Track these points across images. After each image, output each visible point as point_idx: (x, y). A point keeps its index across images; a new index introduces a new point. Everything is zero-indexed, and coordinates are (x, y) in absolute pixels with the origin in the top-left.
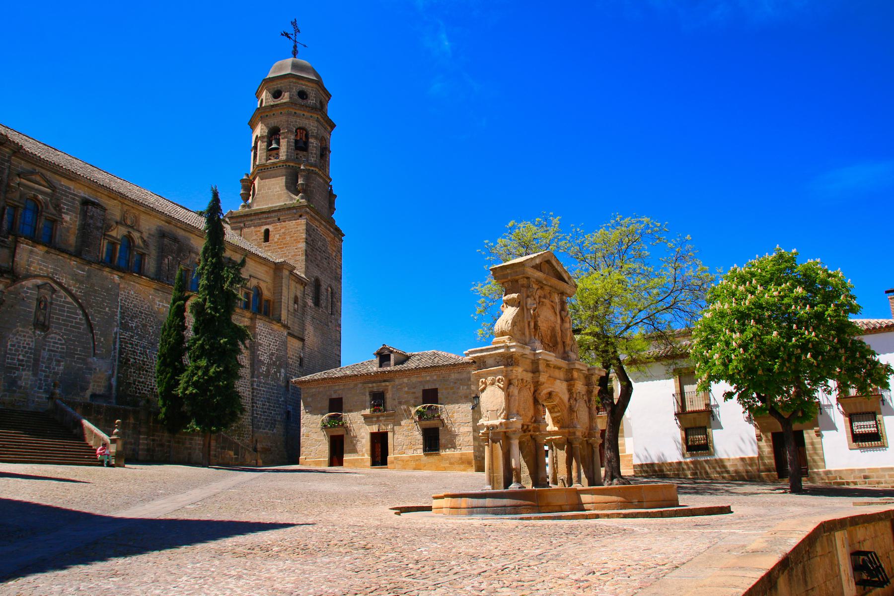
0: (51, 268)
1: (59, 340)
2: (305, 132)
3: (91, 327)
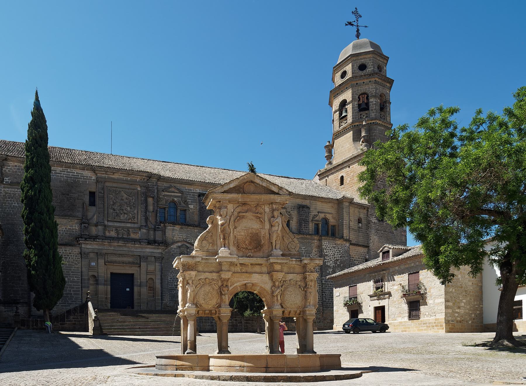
0: (185, 236)
2: (366, 96)
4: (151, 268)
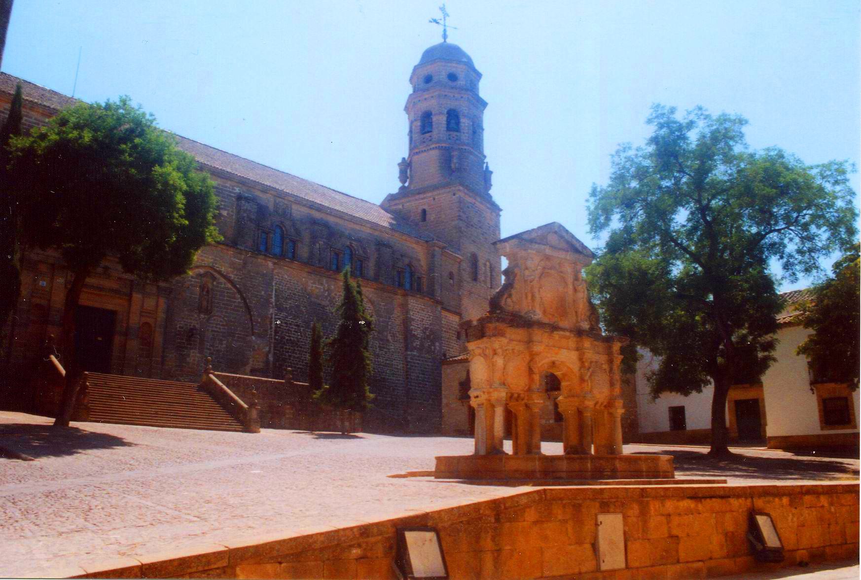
0: (212, 259)
1: (221, 321)
3: (248, 309)
4: (150, 303)
